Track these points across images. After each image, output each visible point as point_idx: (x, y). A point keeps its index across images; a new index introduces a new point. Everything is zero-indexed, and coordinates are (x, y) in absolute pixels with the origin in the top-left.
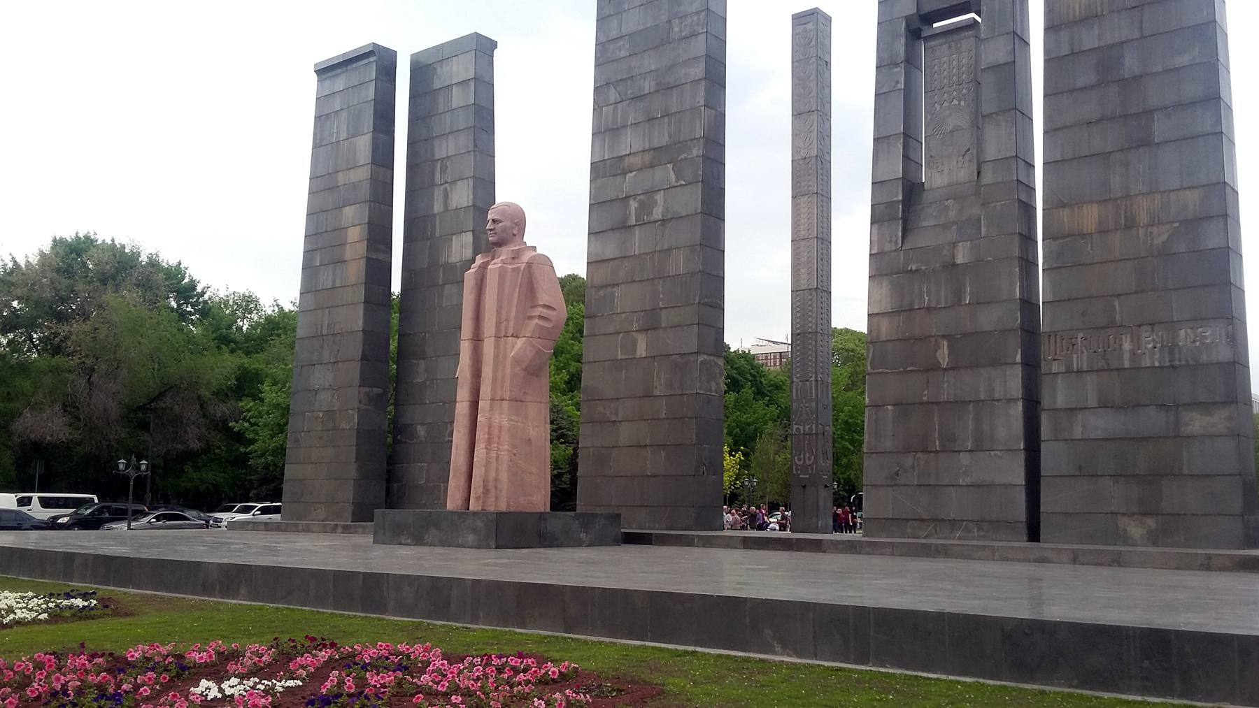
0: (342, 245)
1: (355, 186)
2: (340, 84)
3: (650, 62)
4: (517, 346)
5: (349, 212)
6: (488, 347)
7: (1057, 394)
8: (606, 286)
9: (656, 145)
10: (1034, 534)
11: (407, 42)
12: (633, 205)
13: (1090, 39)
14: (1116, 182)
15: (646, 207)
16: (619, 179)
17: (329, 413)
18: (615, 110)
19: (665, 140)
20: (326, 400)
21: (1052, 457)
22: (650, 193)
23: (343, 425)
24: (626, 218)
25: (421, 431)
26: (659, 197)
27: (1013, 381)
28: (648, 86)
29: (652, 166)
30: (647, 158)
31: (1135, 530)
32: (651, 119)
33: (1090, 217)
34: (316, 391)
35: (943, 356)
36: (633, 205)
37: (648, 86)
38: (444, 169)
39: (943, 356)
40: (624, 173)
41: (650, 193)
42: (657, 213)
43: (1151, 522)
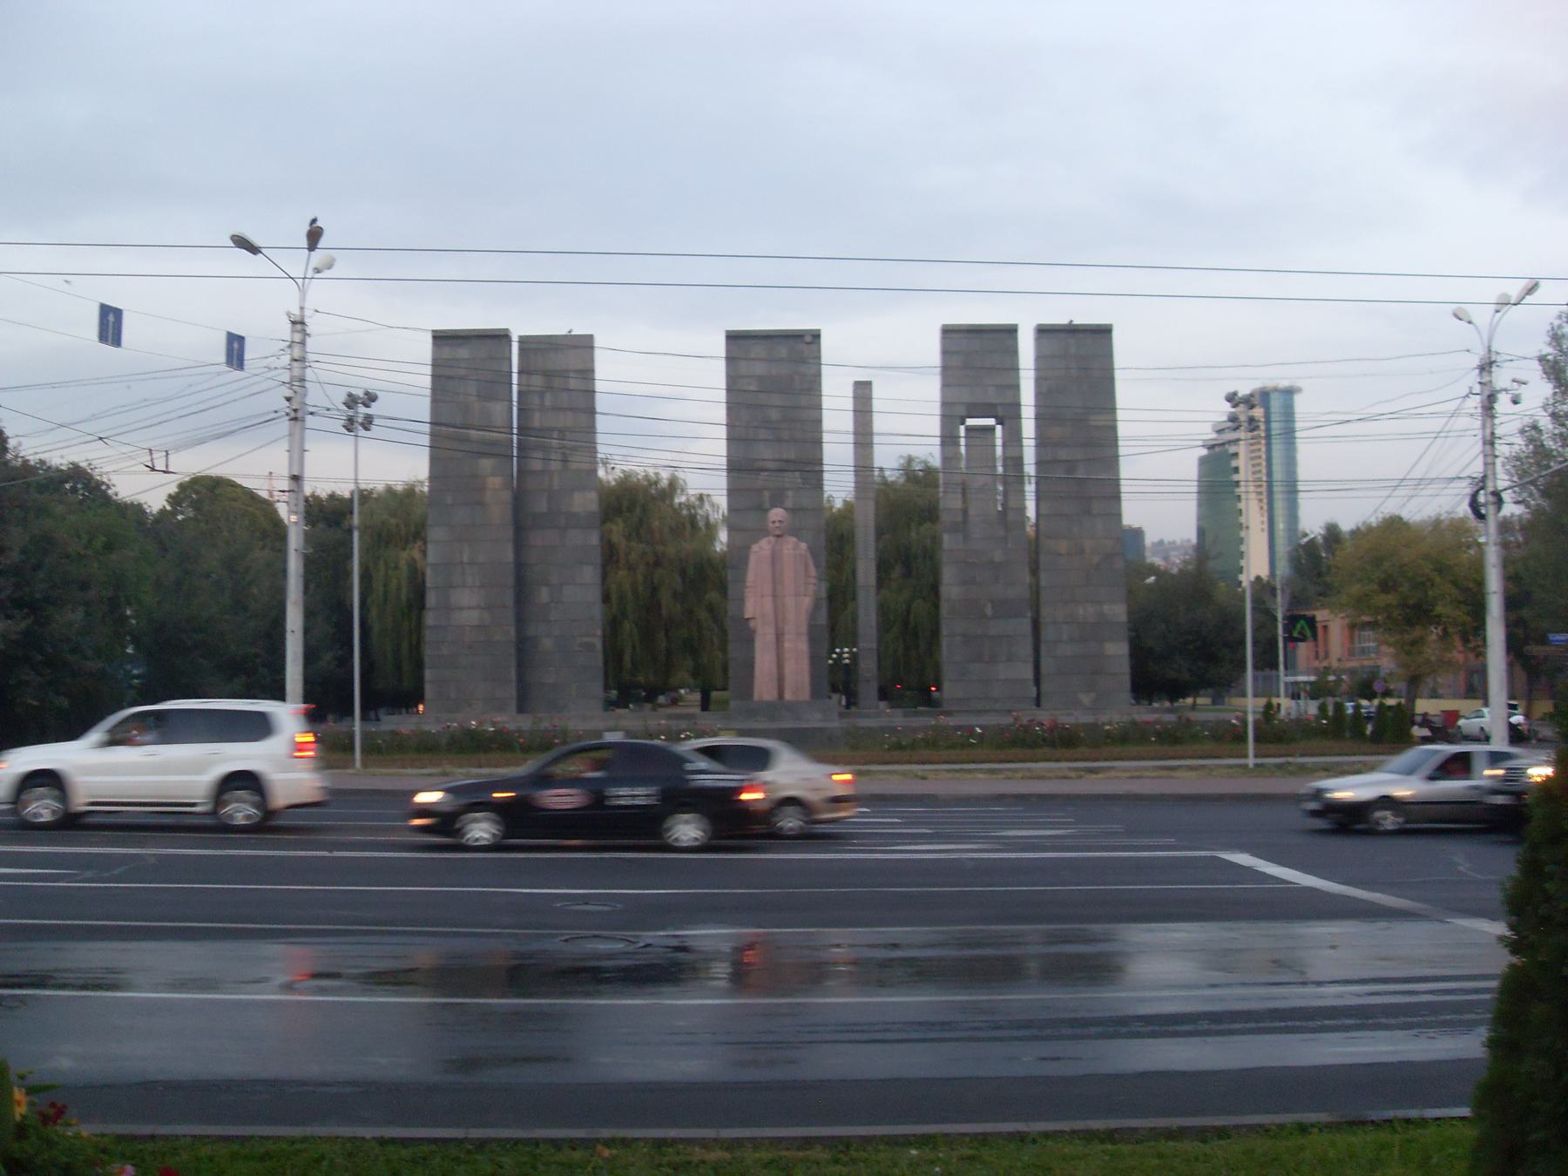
2: (463, 352)
3: (776, 400)
4: (807, 602)
5: (486, 464)
6: (790, 602)
7: (1048, 634)
9: (785, 456)
10: (1038, 702)
11: (524, 323)
12: (766, 494)
13: (1063, 454)
19: (792, 456)
20: (470, 617)
21: (1047, 665)
25: (547, 643)
26: (790, 493)
27: (1025, 625)
31: (1086, 699)
32: (779, 440)
33: (1063, 546)
34: (461, 609)
35: (989, 611)
36: (766, 494)
37: (775, 415)
39: (989, 611)
43: (1093, 695)
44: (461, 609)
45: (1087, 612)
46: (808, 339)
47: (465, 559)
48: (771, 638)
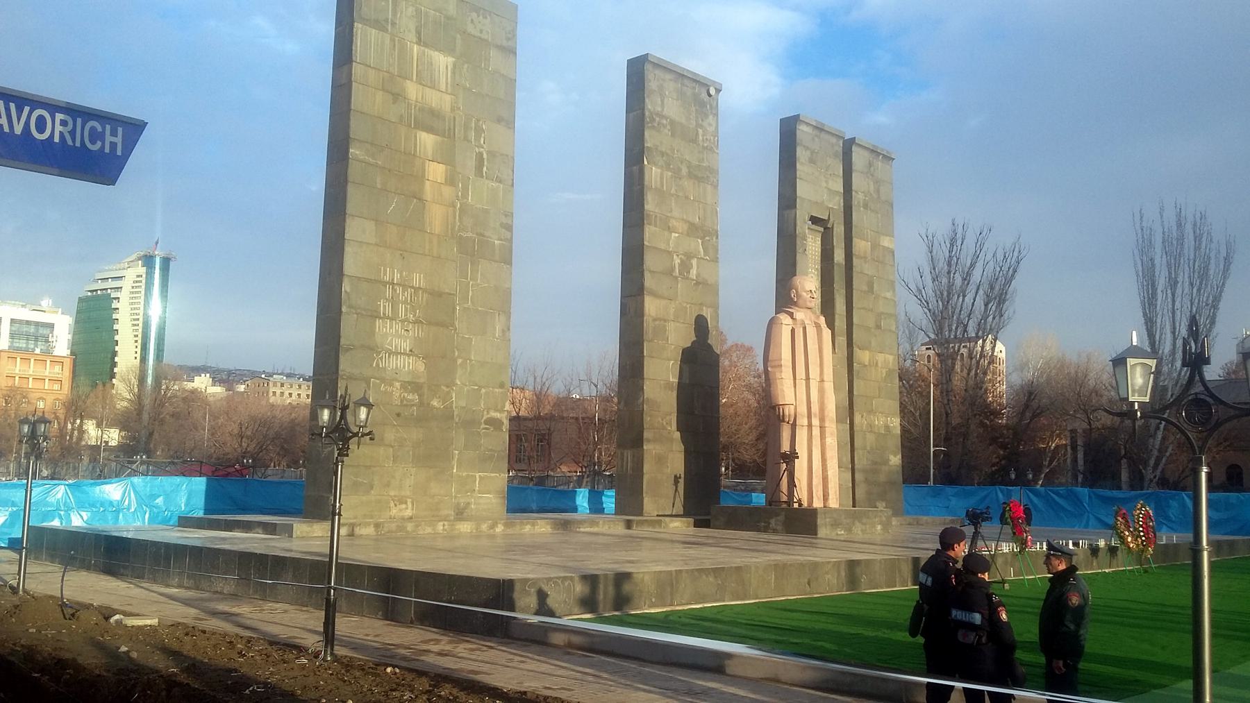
0: (421, 178)
1: (435, 114)
5: (427, 141)
8: (660, 319)
14: (873, 344)
15: (685, 267)
16: (666, 233)
17: (415, 387)
18: (662, 178)
22: (689, 256)
23: (435, 403)
24: (673, 269)
26: (694, 262)
28: (684, 171)
29: (688, 235)
30: (686, 227)
34: (391, 353)
37: (684, 171)
38: (479, 131)
40: (670, 230)
41: (689, 256)
42: (693, 273)
44: (391, 353)
45: (879, 421)
46: (712, 92)
47: (397, 277)
48: (816, 432)
